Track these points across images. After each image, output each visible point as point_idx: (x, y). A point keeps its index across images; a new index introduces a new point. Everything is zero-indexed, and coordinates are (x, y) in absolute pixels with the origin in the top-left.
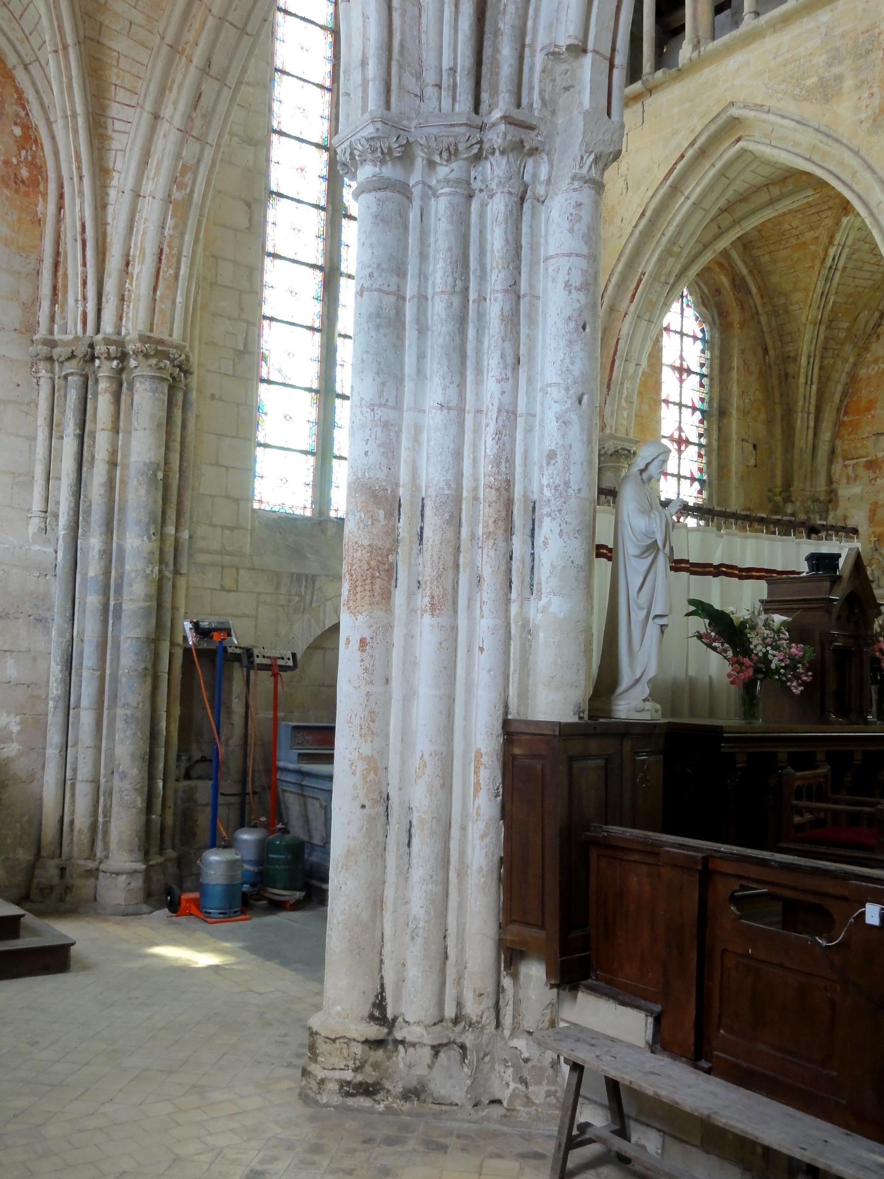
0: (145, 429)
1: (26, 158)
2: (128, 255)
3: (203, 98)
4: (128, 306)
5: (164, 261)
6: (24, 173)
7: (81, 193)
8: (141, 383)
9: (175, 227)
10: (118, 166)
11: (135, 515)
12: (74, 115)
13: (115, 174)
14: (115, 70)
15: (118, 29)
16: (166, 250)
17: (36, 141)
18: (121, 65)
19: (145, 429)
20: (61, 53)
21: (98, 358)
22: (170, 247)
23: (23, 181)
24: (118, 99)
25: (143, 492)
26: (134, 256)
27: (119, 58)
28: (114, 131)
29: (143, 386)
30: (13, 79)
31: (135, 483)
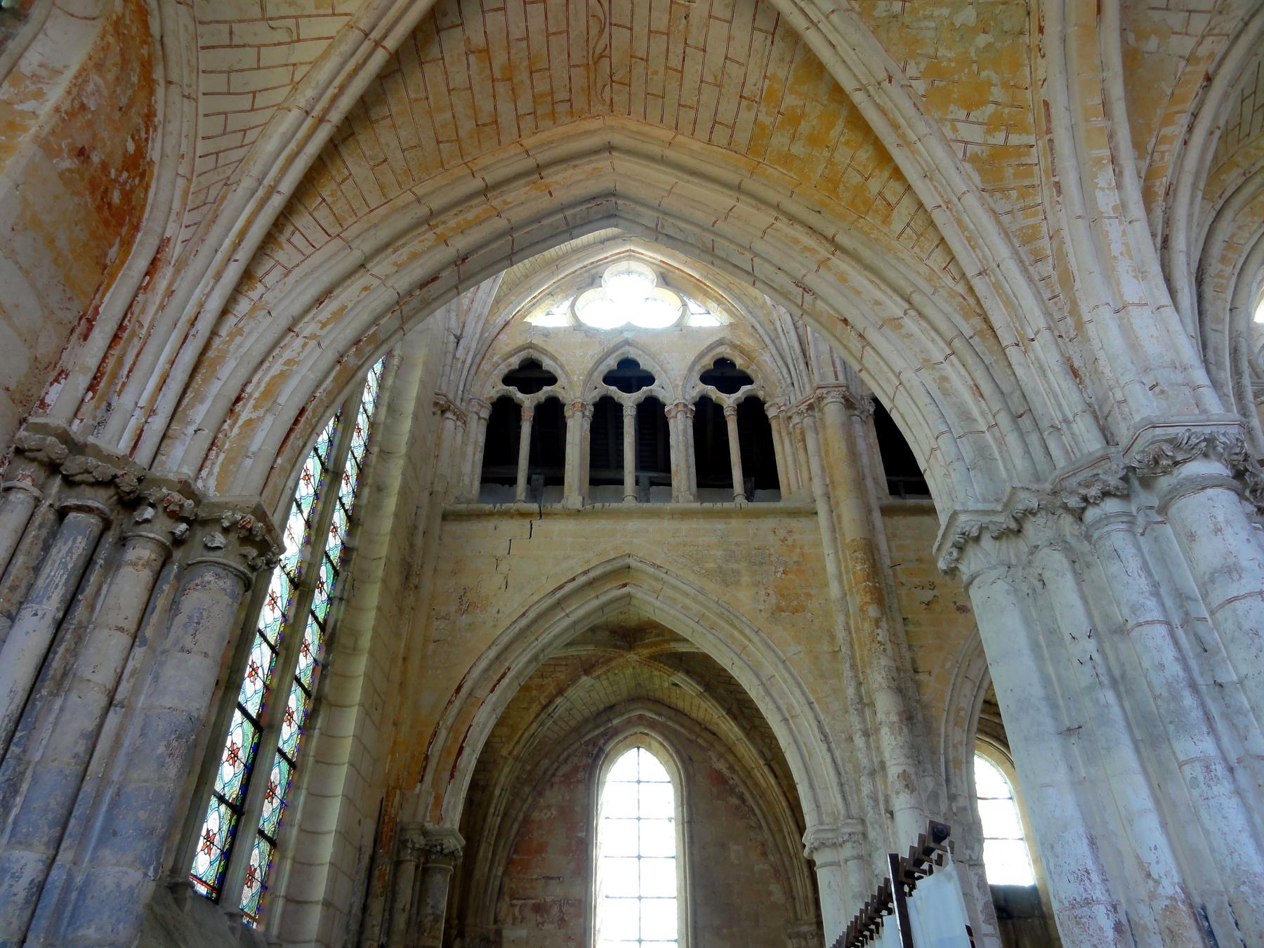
0: (206, 655)
1: (125, 182)
2: (243, 391)
3: (437, 283)
4: (217, 456)
5: (301, 425)
6: (116, 197)
7: (218, 276)
8: (218, 576)
9: (329, 393)
10: (270, 280)
11: (142, 815)
12: (272, 190)
13: (259, 285)
14: (334, 186)
15: (367, 154)
16: (308, 414)
17: (143, 175)
18: (343, 187)
19: (206, 655)
20: (309, 122)
21: (153, 506)
22: (314, 411)
23: (110, 205)
24: (315, 214)
25: (172, 771)
26: (250, 395)
27: (346, 179)
28: (289, 241)
29: (221, 583)
30: (152, 92)
31: (161, 750)
